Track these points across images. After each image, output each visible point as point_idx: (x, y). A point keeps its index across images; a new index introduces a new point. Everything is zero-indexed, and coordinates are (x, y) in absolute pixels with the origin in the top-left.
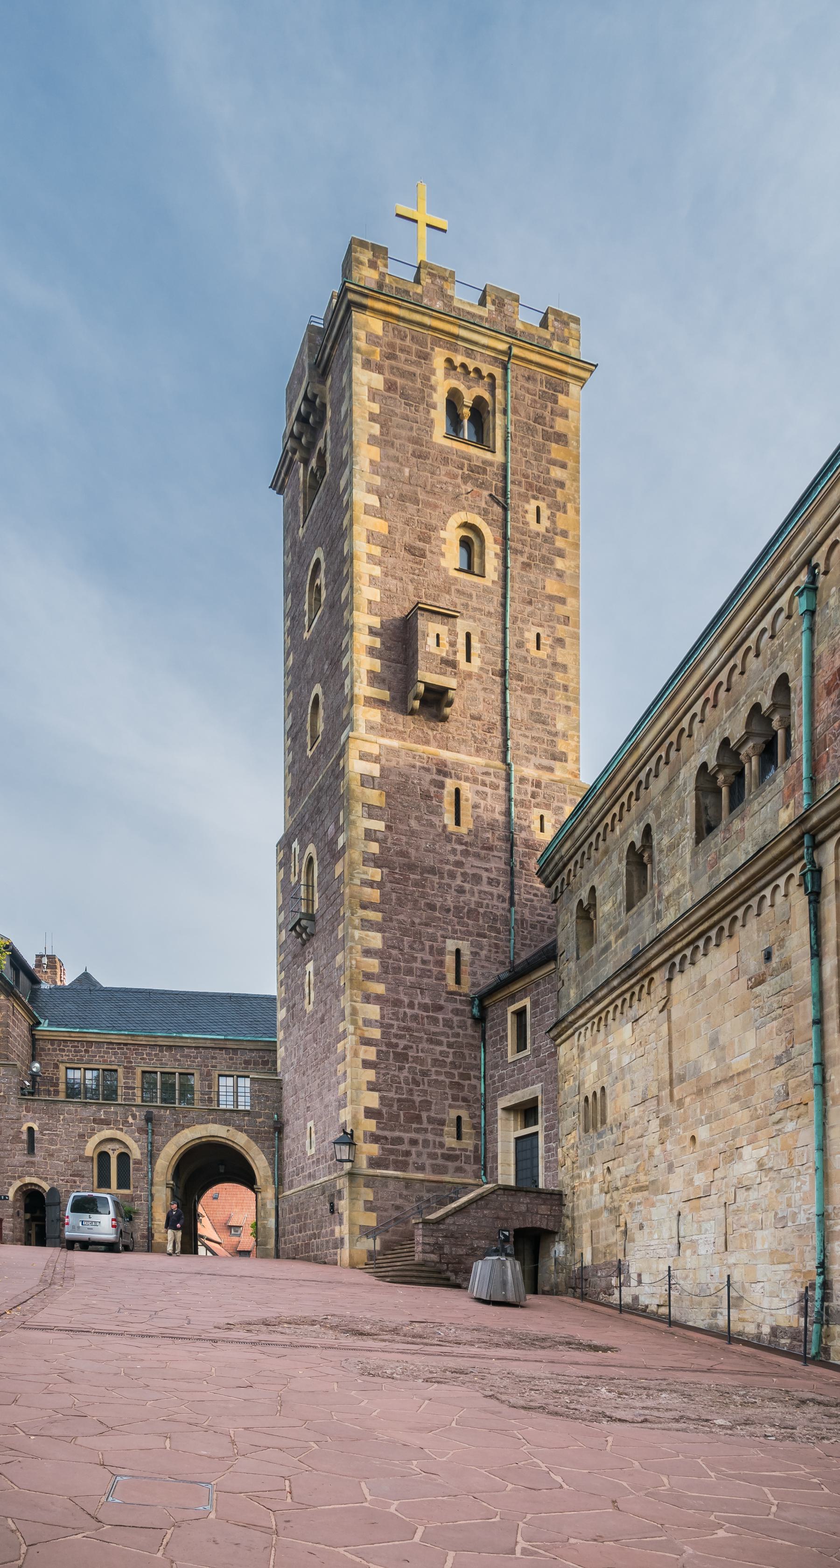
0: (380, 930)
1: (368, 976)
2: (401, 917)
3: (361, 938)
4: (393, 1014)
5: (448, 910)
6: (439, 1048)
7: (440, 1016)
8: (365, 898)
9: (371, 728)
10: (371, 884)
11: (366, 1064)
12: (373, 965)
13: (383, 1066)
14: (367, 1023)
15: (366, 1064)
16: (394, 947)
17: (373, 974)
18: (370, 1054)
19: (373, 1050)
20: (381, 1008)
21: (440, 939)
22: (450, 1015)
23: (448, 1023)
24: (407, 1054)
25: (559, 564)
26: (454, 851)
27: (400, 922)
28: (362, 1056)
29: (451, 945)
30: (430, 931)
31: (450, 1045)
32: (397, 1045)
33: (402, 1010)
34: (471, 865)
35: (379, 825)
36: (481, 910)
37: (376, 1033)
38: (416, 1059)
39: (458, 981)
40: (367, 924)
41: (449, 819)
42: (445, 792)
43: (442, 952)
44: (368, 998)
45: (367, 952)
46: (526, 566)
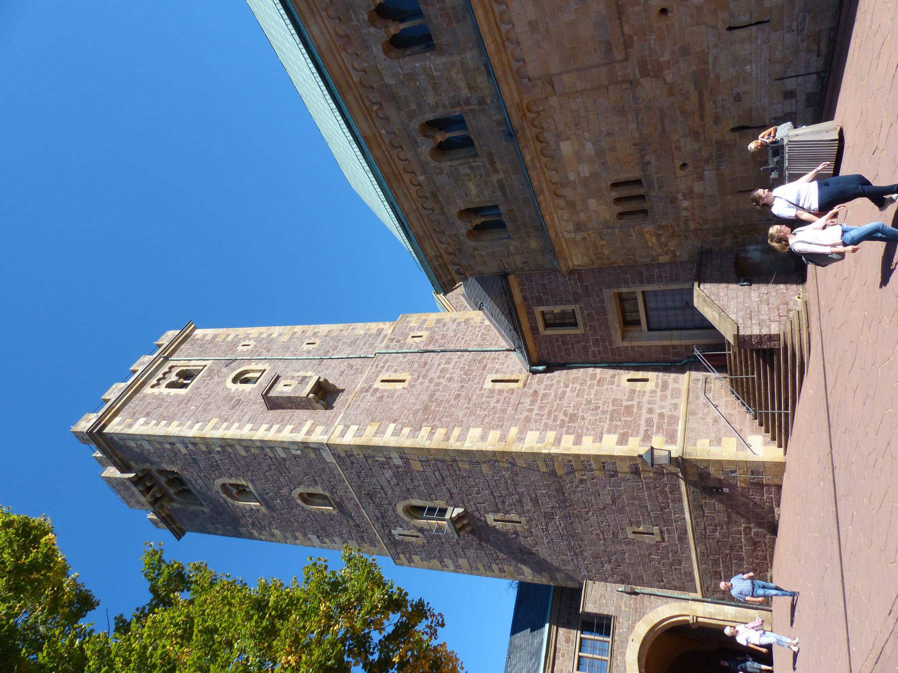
0: (468, 429)
1: (503, 438)
2: (461, 415)
3: (471, 442)
4: (536, 422)
5: (462, 387)
6: (568, 393)
7: (542, 392)
8: (442, 437)
10: (432, 433)
11: (578, 442)
13: (580, 431)
14: (541, 440)
15: (578, 442)
16: (483, 421)
17: (501, 435)
19: (565, 437)
20: (531, 430)
21: (482, 392)
22: (542, 386)
24: (571, 415)
25: (274, 336)
26: (421, 383)
27: (465, 416)
28: (570, 445)
29: (488, 385)
30: (475, 397)
31: (567, 386)
32: (563, 421)
33: (534, 417)
35: (392, 426)
36: (467, 367)
38: (577, 407)
39: (516, 381)
42: (381, 388)
43: (492, 391)
44: (521, 439)
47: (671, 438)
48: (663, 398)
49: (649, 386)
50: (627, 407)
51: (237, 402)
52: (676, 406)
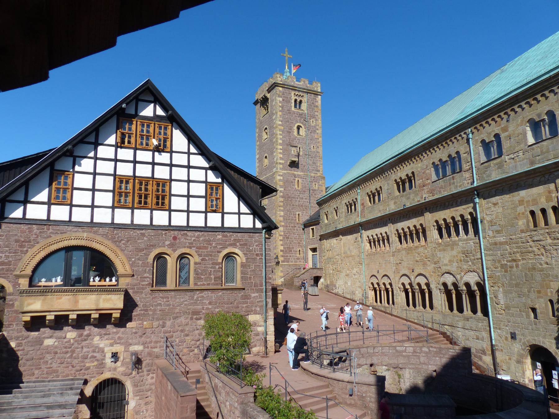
1: (281, 221)
9: (280, 169)
11: (281, 240)
12: (282, 219)
15: (281, 240)
18: (281, 238)
23: (297, 230)
25: (317, 131)
29: (297, 213)
34: (301, 196)
37: (282, 233)
38: (291, 238)
40: (280, 210)
41: (296, 186)
43: (295, 215)
45: (280, 216)
46: (311, 133)
47: (283, 262)
48: (294, 259)
49: (298, 255)
50: (291, 251)
51: (290, 132)
52: (292, 262)
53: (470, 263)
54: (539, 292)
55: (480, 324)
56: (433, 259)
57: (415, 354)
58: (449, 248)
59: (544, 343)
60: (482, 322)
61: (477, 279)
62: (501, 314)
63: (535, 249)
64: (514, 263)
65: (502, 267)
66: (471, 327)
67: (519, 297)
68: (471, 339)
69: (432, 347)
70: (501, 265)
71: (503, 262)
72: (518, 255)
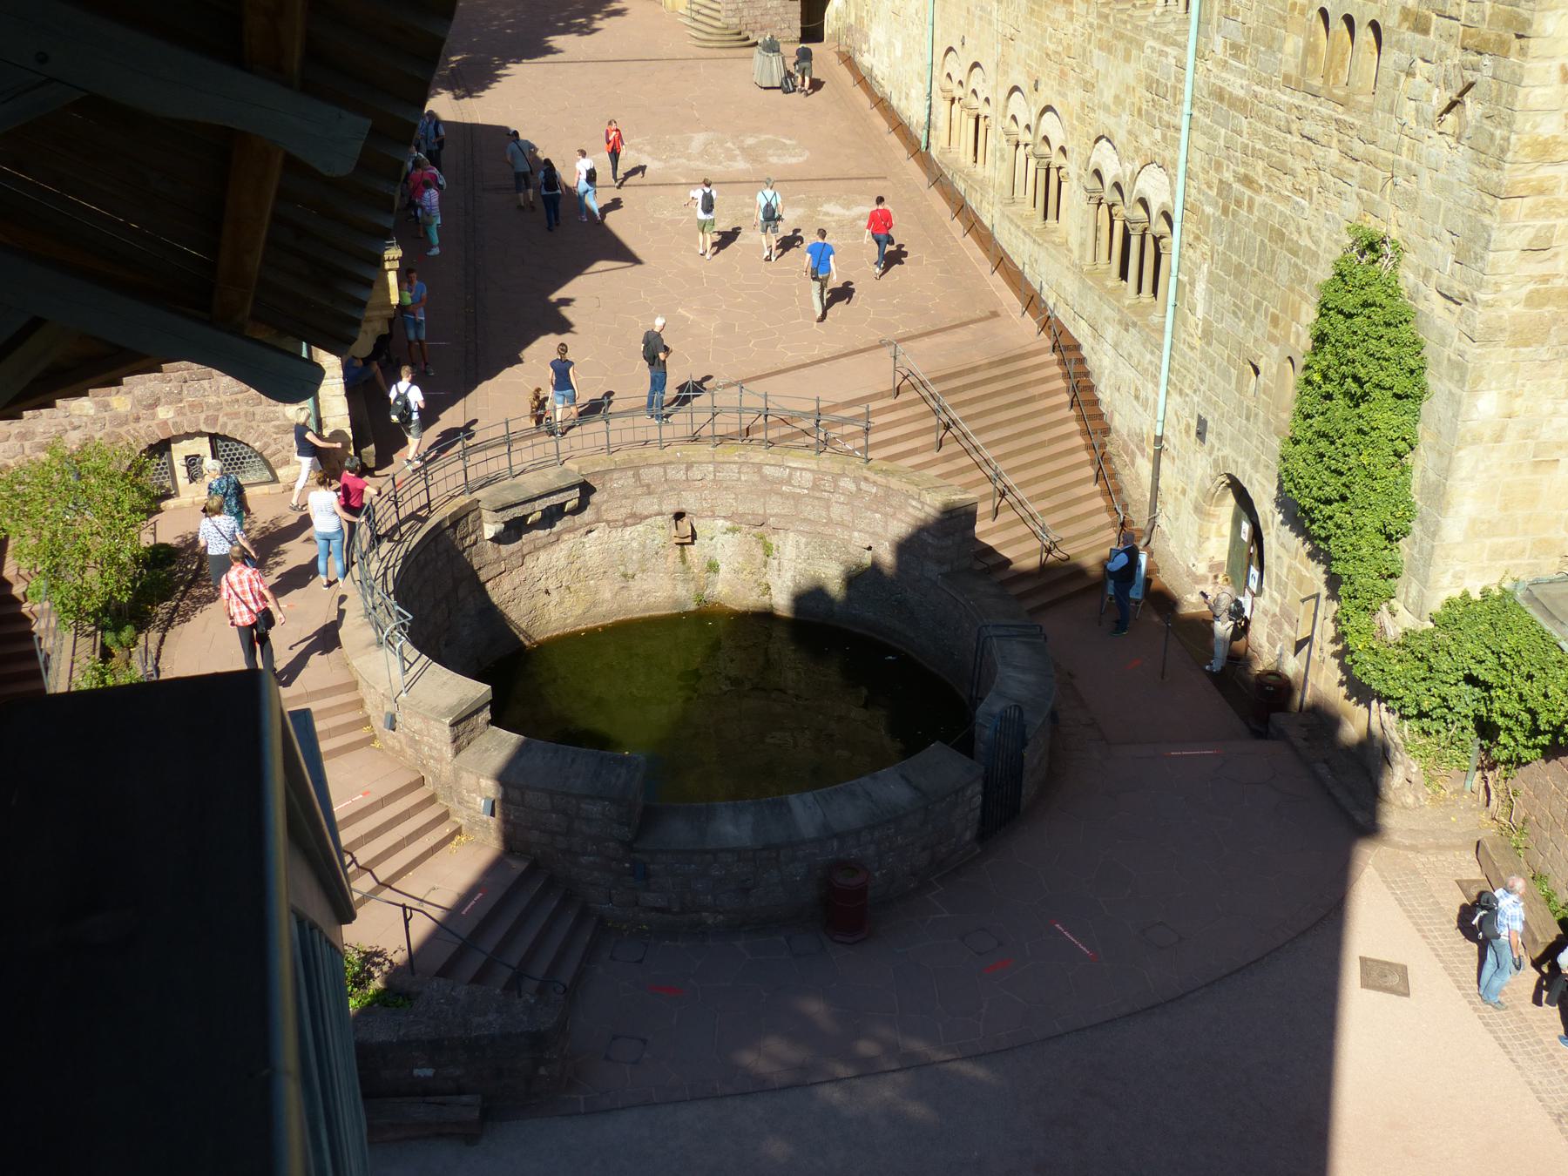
53: (1158, 134)
54: (1275, 321)
55: (1148, 356)
56: (1083, 70)
57: (817, 494)
58: (1121, 45)
59: (1250, 481)
60: (1152, 353)
61: (1166, 198)
62: (1192, 348)
63: (1298, 165)
64: (1248, 193)
65: (1219, 194)
66: (1130, 355)
67: (1234, 313)
68: (1124, 390)
69: (866, 479)
70: (1221, 181)
71: (1228, 176)
72: (1260, 165)
